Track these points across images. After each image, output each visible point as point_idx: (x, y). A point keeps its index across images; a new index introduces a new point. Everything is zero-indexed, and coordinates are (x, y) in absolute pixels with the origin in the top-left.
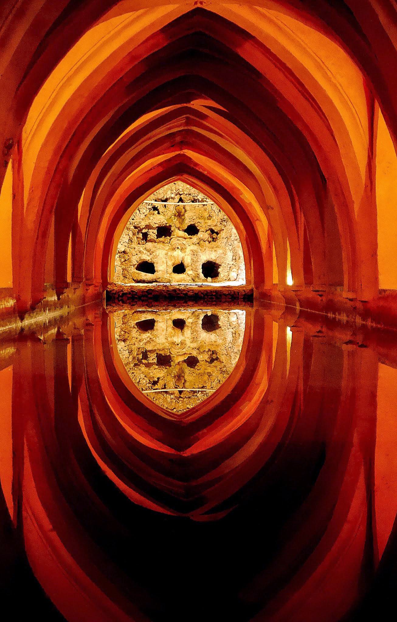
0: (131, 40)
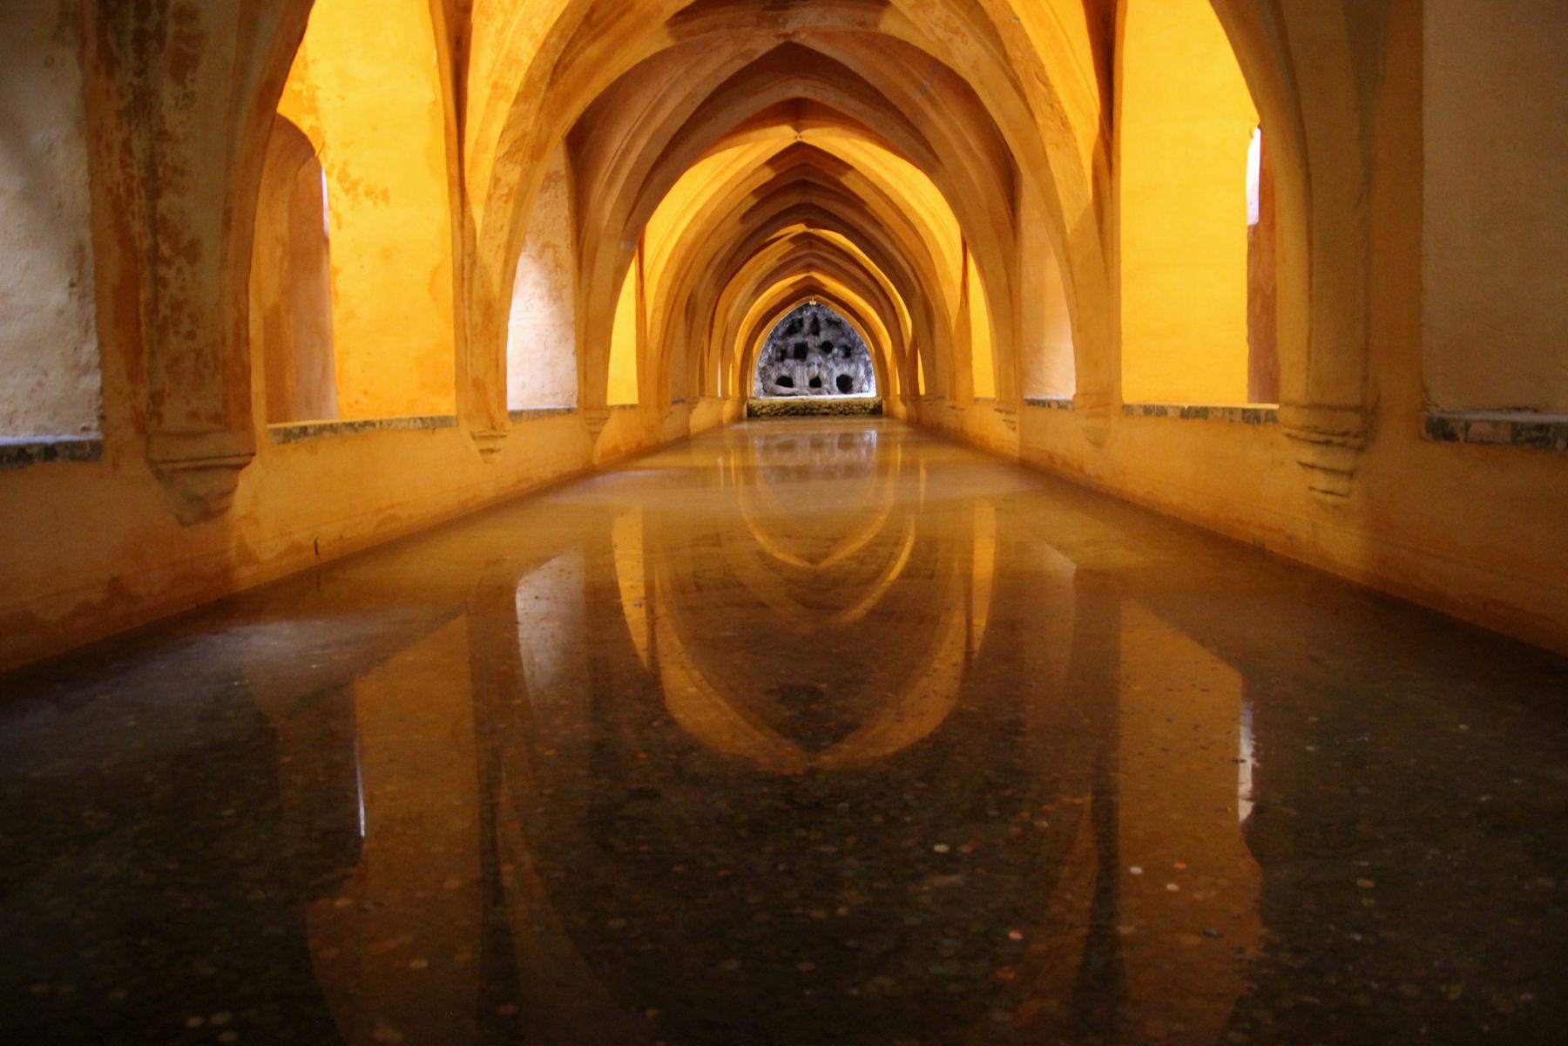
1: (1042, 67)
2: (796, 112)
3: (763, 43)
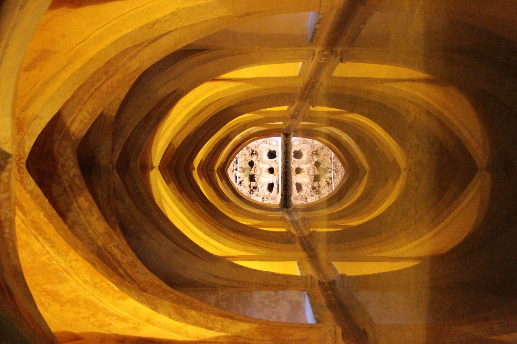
0: (173, 201)
1: (146, 25)
2: (145, 168)
3: (116, 179)
